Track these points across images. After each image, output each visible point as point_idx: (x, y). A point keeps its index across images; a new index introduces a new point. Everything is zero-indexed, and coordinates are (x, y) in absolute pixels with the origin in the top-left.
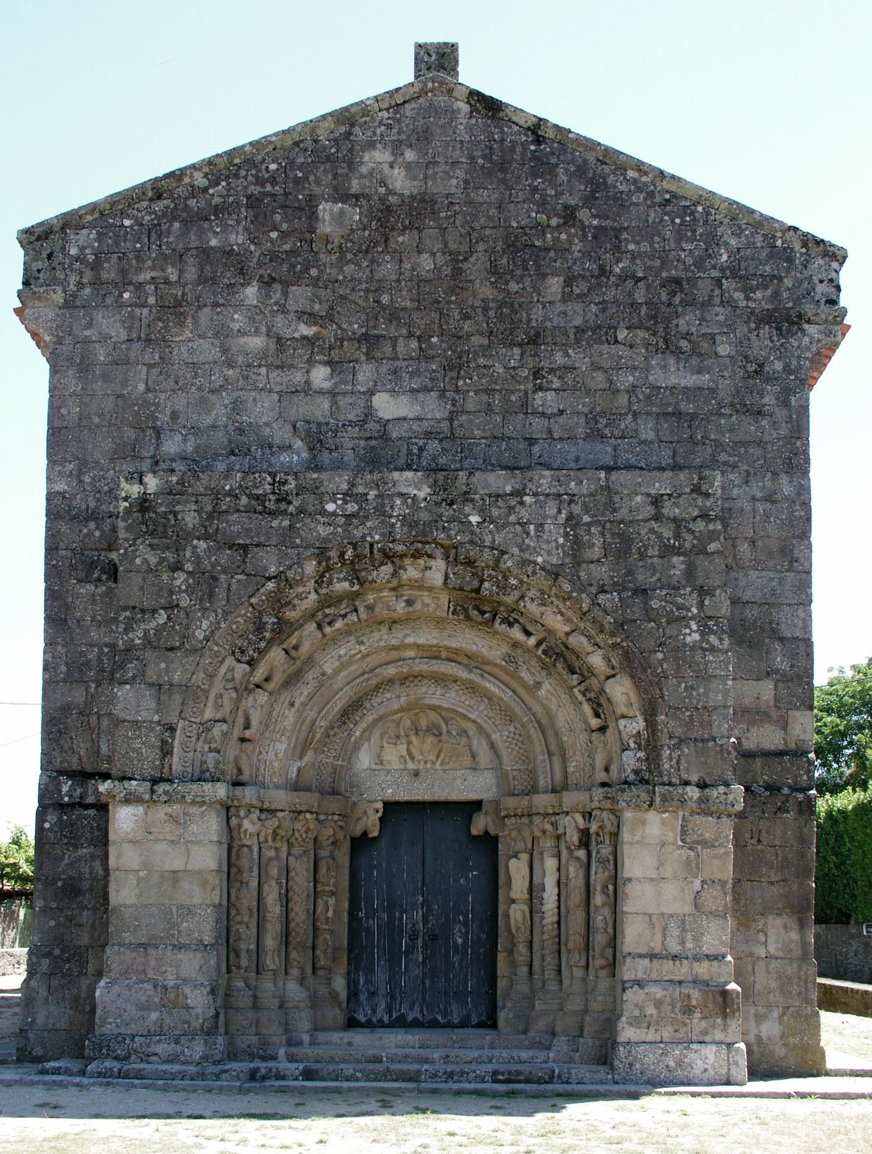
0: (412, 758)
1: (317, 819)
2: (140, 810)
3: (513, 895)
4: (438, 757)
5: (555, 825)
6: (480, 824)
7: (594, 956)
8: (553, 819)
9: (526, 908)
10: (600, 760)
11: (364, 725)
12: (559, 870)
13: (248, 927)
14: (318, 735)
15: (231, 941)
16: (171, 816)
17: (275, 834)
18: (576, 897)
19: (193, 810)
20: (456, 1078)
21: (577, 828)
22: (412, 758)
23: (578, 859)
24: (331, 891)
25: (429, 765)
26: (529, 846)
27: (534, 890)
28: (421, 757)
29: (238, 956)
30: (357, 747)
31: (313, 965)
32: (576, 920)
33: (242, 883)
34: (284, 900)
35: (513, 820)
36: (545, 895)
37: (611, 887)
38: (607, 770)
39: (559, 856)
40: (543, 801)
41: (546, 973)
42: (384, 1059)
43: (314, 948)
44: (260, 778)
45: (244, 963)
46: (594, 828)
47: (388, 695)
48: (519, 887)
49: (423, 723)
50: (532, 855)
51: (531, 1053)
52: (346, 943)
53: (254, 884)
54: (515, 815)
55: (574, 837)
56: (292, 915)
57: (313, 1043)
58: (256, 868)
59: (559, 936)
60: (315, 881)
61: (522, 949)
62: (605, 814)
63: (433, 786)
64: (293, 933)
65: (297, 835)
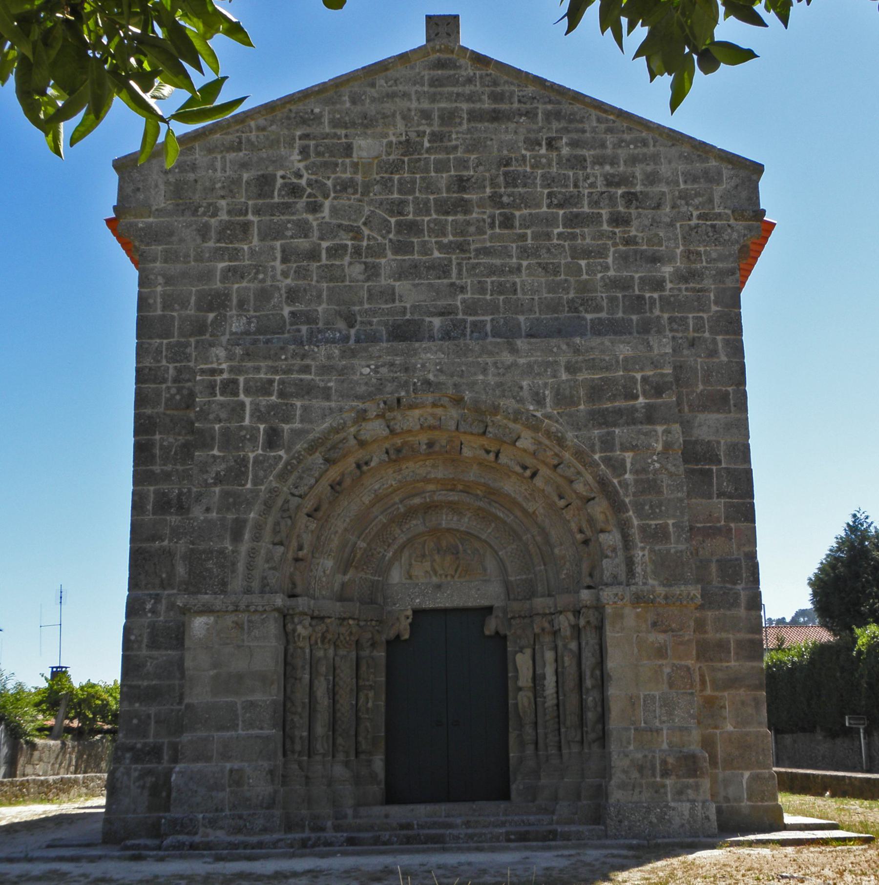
0: (435, 573)
1: (358, 625)
2: (212, 619)
3: (521, 683)
4: (456, 571)
5: (551, 623)
6: (491, 626)
7: (587, 732)
8: (550, 618)
9: (530, 695)
10: (585, 567)
11: (396, 547)
12: (556, 661)
13: (301, 717)
14: (358, 556)
15: (287, 729)
16: (237, 623)
17: (323, 638)
18: (570, 683)
19: (255, 618)
20: (475, 839)
21: (570, 625)
22: (435, 573)
23: (571, 650)
24: (371, 686)
25: (449, 578)
26: (532, 642)
27: (537, 679)
29: (293, 742)
30: (391, 563)
31: (356, 749)
32: (572, 702)
33: (296, 679)
34: (331, 694)
35: (518, 621)
36: (546, 683)
37: (598, 672)
38: (591, 575)
39: (556, 649)
40: (540, 603)
41: (549, 748)
42: (416, 826)
43: (356, 735)
44: (311, 591)
45: (298, 747)
46: (582, 622)
47: (414, 522)
48: (525, 678)
49: (444, 544)
50: (534, 649)
51: (538, 817)
52: (383, 729)
53: (307, 677)
54: (520, 617)
55: (566, 631)
56: (338, 706)
57: (355, 816)
58: (307, 667)
59: (558, 717)
60: (357, 677)
61: (529, 729)
62: (591, 612)
64: (339, 722)
65: (342, 638)
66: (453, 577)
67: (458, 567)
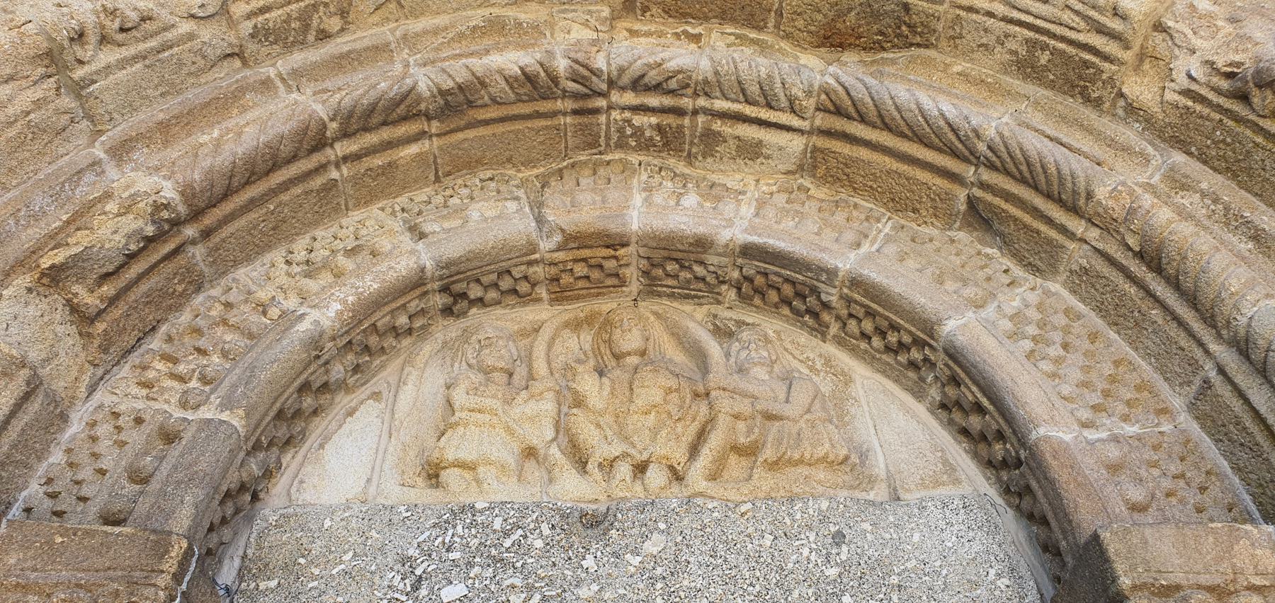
0: (581, 464)
4: (694, 450)
25: (656, 477)
28: (617, 449)
63: (678, 566)
66: (677, 476)
67: (702, 436)
